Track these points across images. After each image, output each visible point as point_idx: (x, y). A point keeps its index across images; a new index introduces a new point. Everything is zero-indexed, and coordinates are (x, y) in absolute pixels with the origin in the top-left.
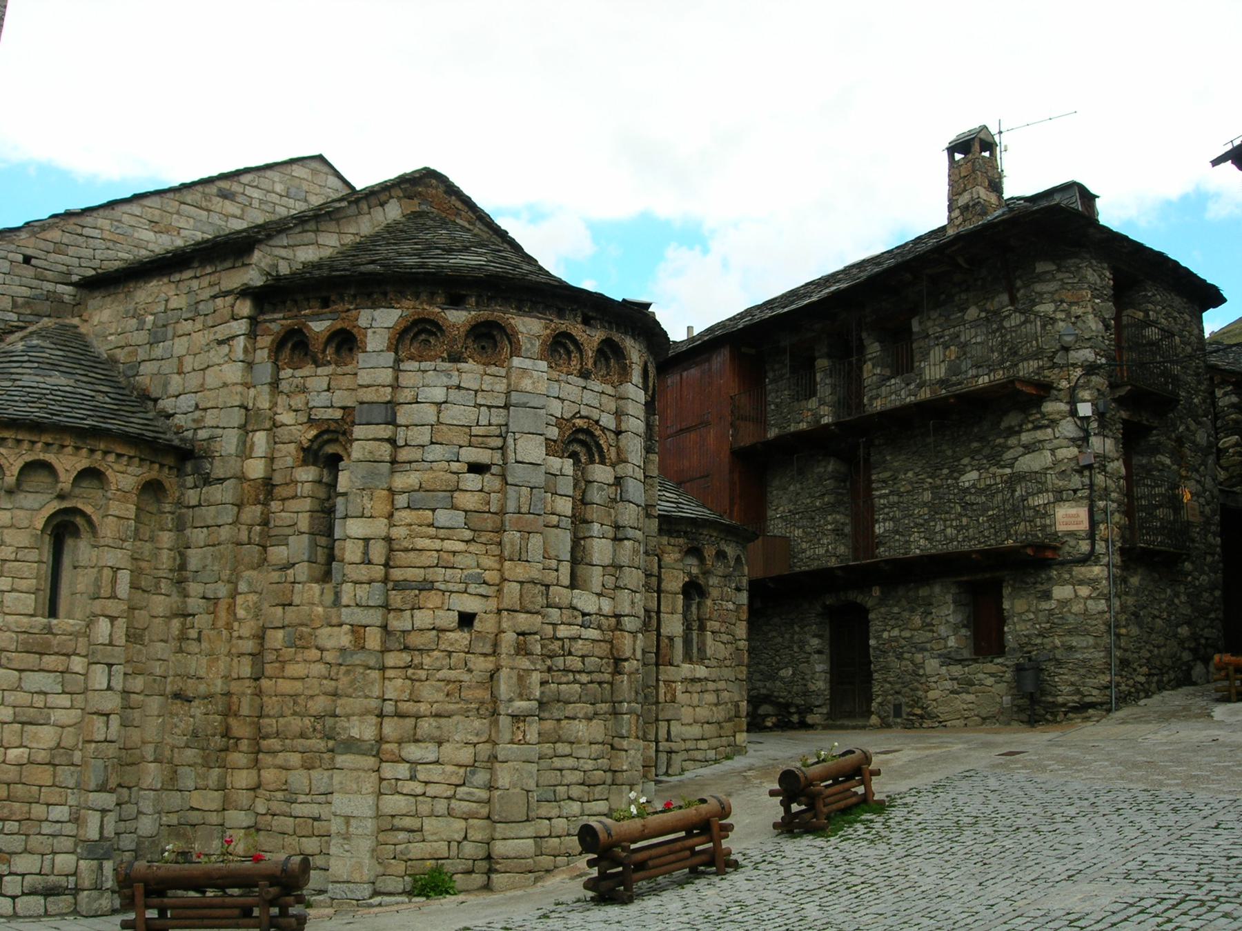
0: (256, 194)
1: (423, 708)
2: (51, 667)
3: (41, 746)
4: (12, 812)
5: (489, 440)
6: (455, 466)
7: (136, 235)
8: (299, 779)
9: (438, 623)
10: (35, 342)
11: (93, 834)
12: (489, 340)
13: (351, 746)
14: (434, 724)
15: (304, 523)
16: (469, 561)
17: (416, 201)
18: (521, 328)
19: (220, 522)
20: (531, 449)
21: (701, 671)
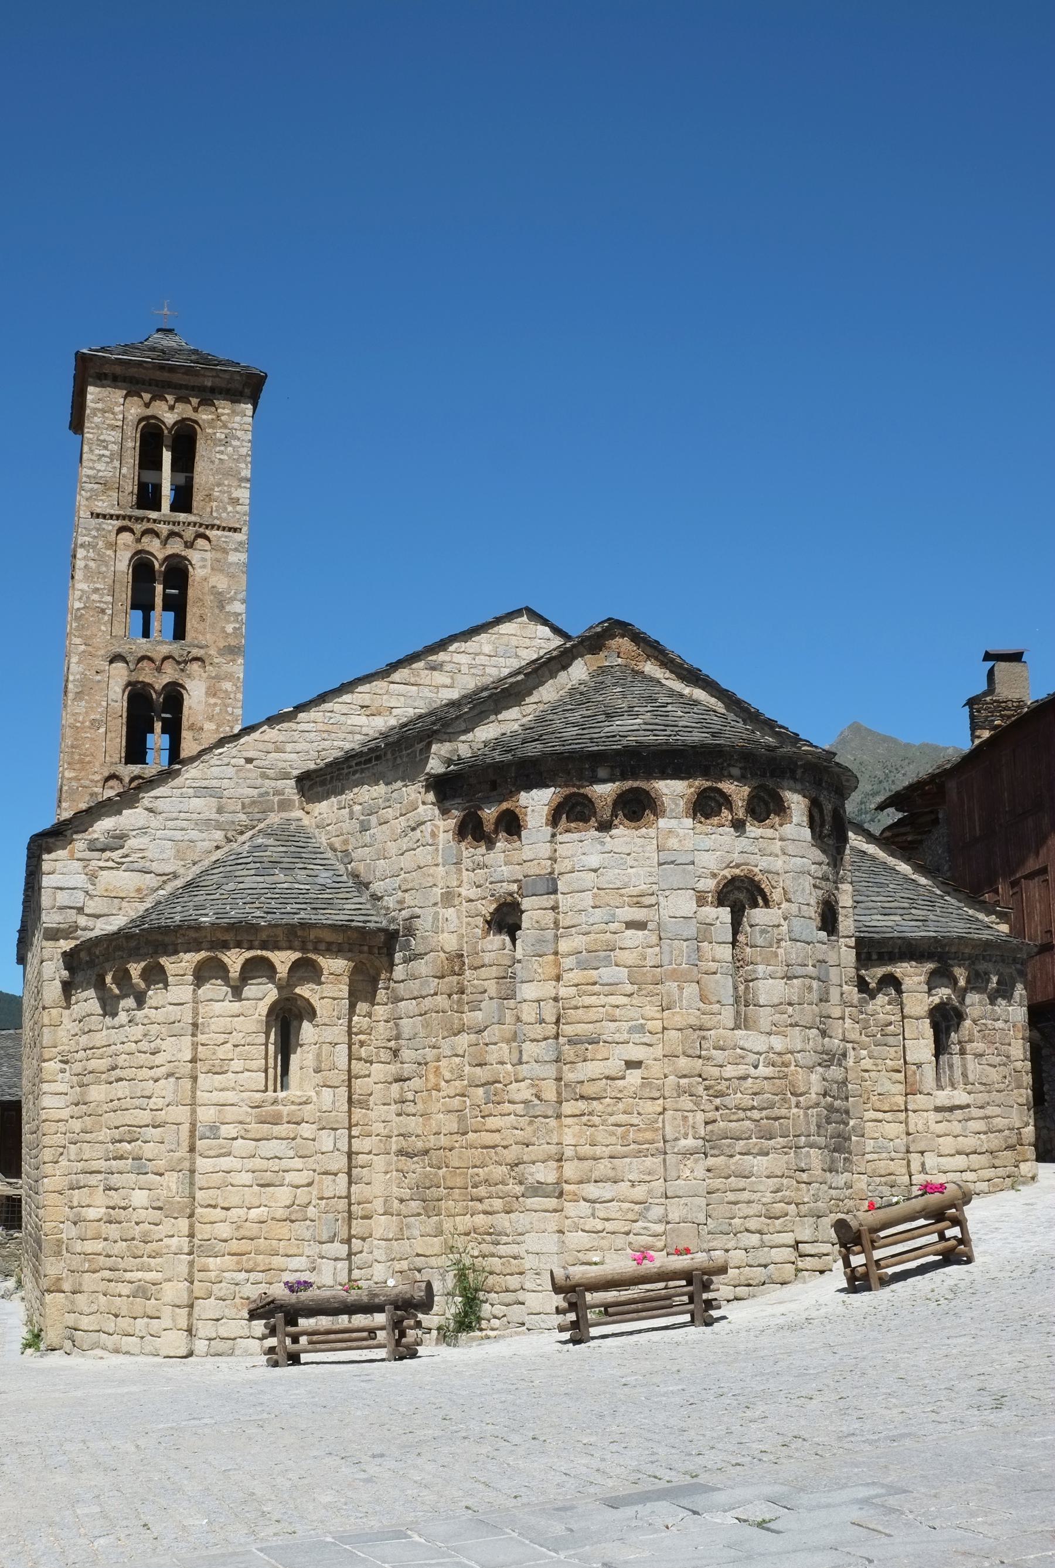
0: (463, 659)
1: (598, 1150)
2: (283, 1135)
3: (279, 1205)
4: (256, 1264)
5: (643, 899)
6: (613, 927)
7: (349, 722)
8: (502, 1221)
9: (607, 1072)
10: (260, 841)
12: (637, 807)
13: (537, 1190)
14: (610, 1165)
15: (492, 987)
16: (633, 1013)
18: (665, 791)
19: (424, 993)
20: (685, 904)
21: (960, 1097)
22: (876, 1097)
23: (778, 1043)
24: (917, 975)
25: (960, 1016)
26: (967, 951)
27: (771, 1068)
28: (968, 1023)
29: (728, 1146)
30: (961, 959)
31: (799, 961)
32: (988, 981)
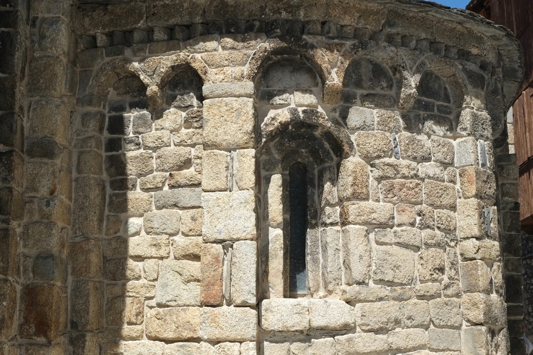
22: (153, 312)
24: (233, 63)
25: (339, 150)
26: (347, 20)
28: (352, 163)
30: (334, 37)
32: (401, 83)
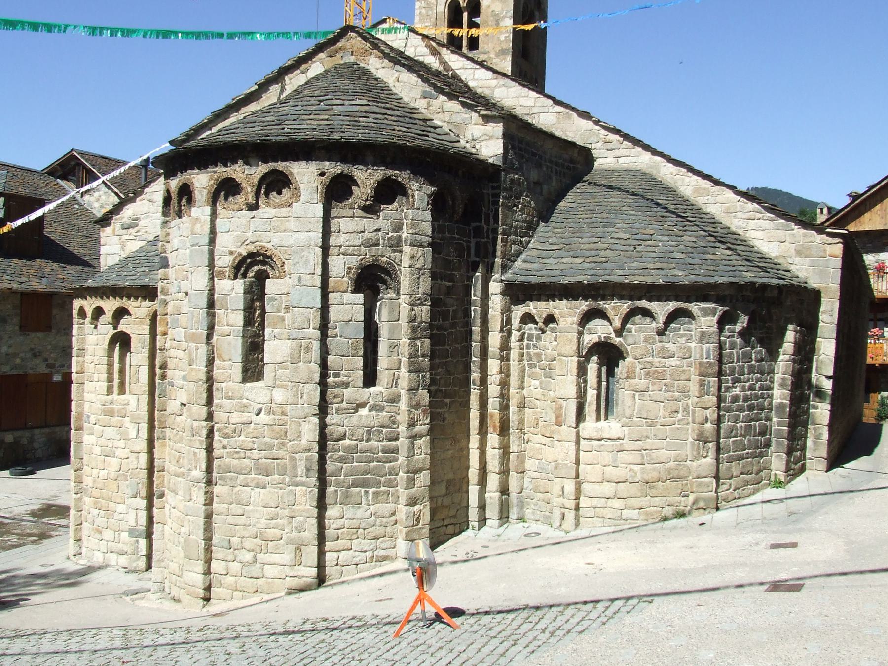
11: (132, 523)
17: (339, 55)
23: (279, 396)
27: (272, 416)
29: (231, 479)
31: (296, 325)
